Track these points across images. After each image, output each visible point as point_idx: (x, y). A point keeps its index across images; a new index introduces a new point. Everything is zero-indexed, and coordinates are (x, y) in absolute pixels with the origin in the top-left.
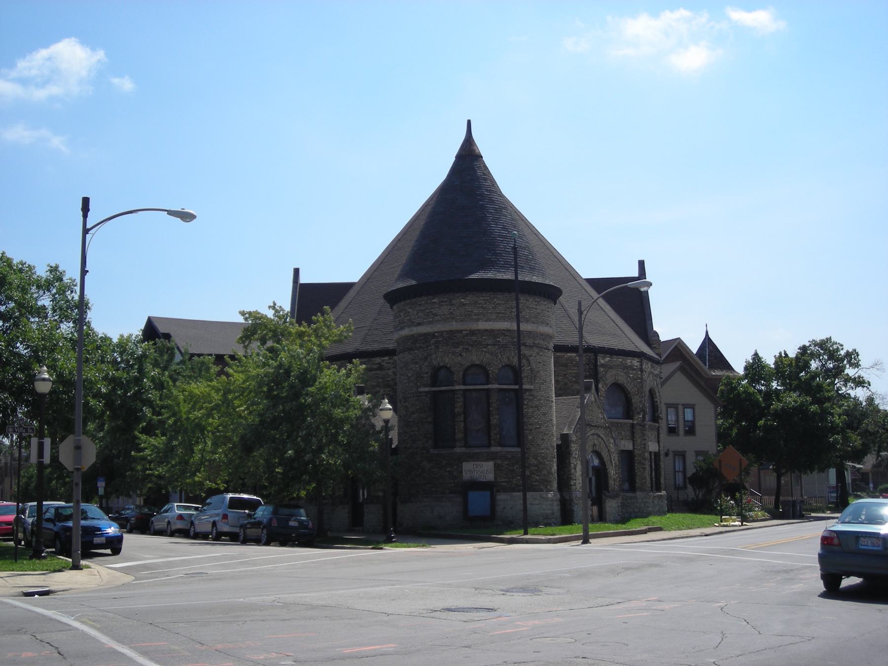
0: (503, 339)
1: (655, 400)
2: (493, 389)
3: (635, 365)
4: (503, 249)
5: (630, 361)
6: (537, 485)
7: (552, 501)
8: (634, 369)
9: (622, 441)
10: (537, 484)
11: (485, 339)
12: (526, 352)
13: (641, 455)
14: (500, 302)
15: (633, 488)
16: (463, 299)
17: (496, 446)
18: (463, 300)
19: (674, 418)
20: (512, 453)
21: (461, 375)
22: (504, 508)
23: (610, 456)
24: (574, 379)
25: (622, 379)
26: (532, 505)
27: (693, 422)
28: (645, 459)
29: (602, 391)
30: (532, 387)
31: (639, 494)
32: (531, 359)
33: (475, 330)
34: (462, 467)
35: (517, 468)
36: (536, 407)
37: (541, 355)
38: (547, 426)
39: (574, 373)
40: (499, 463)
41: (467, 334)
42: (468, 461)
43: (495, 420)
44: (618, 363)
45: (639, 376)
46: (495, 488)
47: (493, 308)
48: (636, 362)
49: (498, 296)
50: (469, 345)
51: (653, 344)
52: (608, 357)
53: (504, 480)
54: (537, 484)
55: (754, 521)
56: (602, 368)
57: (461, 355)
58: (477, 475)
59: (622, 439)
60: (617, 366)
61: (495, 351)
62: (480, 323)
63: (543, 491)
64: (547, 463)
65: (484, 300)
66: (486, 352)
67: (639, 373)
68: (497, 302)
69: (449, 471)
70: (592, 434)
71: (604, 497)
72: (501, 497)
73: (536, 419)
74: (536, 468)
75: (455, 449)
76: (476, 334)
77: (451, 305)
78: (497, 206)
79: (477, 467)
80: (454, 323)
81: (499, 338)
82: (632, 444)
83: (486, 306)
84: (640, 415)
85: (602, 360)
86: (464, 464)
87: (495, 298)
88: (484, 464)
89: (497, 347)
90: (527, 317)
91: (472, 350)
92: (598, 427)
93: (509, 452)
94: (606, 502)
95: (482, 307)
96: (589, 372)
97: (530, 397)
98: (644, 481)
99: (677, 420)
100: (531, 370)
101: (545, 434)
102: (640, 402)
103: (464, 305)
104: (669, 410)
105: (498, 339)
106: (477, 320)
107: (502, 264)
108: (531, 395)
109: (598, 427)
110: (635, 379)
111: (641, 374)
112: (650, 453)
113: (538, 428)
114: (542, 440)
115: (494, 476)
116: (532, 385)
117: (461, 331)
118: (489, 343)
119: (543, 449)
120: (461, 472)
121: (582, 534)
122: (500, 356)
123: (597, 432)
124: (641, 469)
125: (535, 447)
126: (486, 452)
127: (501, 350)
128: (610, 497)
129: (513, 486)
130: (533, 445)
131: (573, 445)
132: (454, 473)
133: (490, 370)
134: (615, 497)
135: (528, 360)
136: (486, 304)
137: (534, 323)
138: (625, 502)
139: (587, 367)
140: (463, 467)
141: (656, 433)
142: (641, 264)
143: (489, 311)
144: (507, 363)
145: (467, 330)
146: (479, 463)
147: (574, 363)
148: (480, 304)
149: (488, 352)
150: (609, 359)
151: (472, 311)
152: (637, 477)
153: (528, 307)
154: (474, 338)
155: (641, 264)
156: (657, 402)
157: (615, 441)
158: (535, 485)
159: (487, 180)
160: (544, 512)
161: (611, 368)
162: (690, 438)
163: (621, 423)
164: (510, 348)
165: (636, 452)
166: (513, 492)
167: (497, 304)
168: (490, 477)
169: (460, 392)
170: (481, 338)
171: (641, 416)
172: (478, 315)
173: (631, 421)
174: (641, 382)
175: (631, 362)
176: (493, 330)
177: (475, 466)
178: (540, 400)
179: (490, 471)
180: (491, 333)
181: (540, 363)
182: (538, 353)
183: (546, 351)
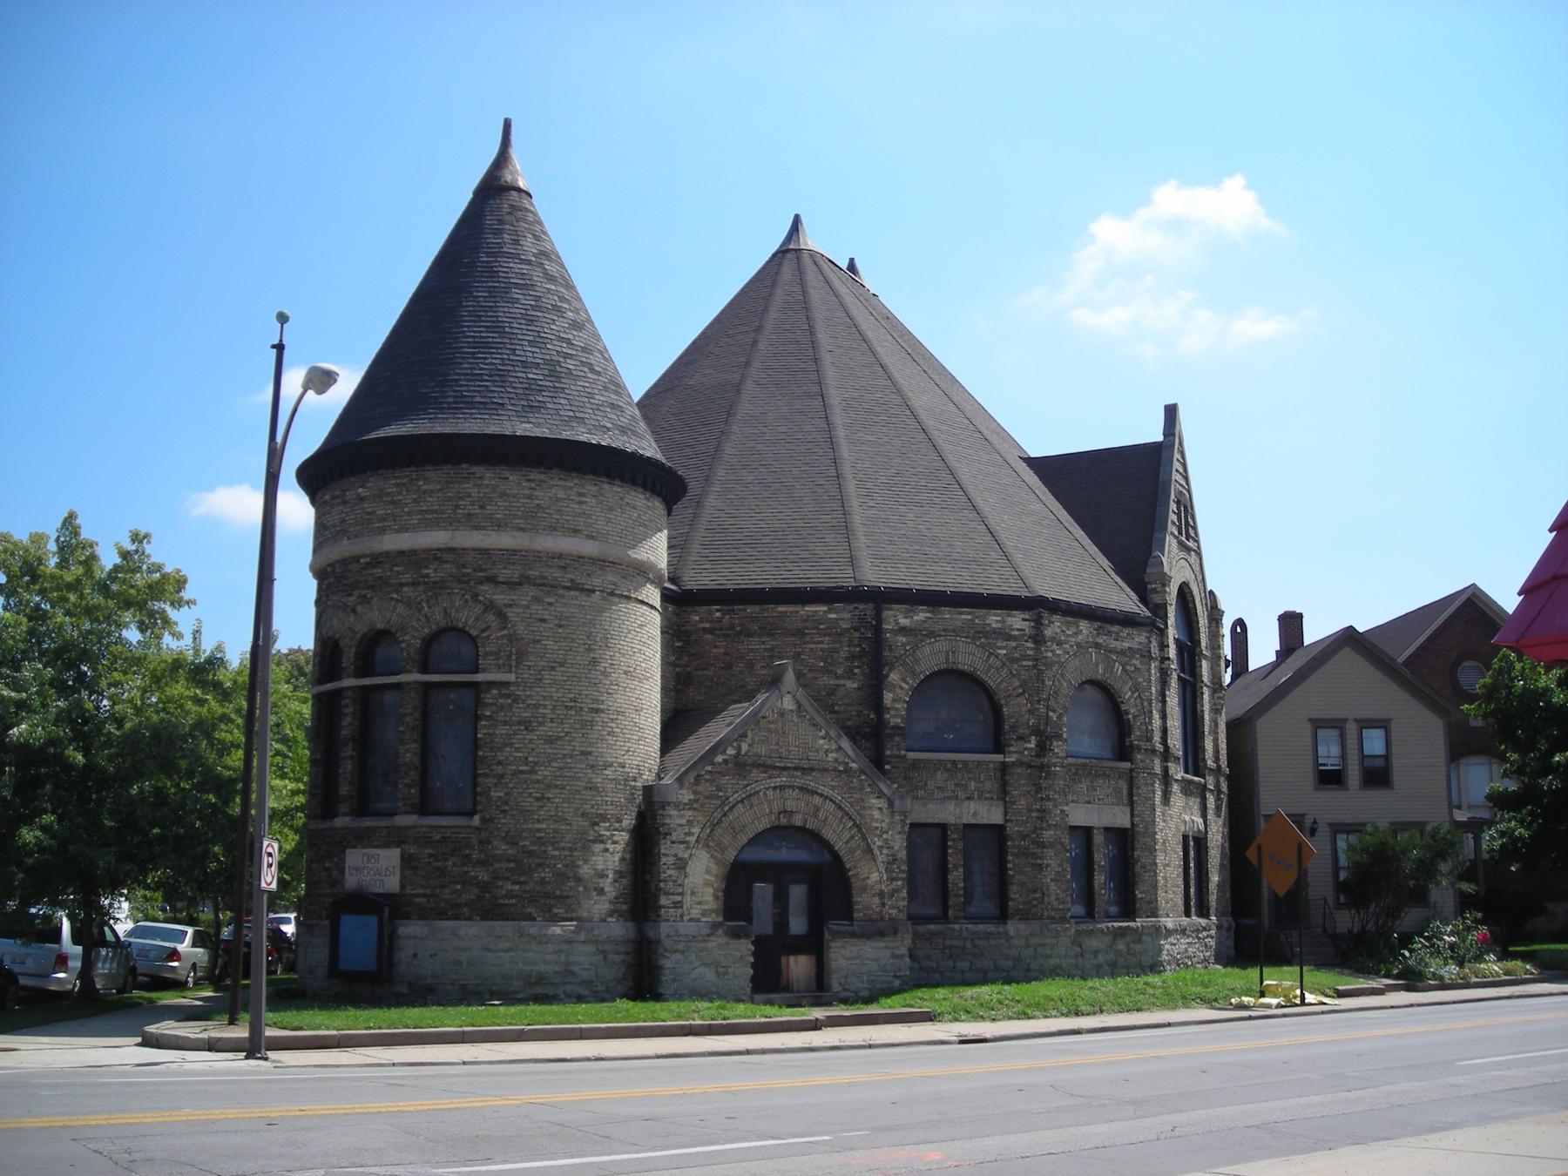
0: (435, 570)
1: (1123, 707)
2: (408, 683)
3: (1016, 627)
4: (469, 371)
5: (999, 618)
6: (511, 905)
7: (570, 942)
8: (1010, 638)
9: (966, 803)
10: (514, 901)
11: (399, 573)
12: (495, 597)
13: (1028, 836)
14: (431, 487)
15: (1003, 916)
16: (360, 487)
17: (408, 813)
18: (360, 490)
19: (1335, 750)
20: (445, 830)
21: (352, 655)
22: (415, 955)
23: (864, 838)
24: (822, 664)
25: (969, 658)
26: (489, 950)
27: (1387, 757)
28: (1042, 845)
29: (901, 688)
30: (511, 677)
31: (1012, 927)
32: (511, 614)
33: (381, 554)
34: (344, 861)
35: (454, 864)
36: (519, 723)
37: (550, 604)
38: (560, 768)
39: (822, 649)
41: (368, 564)
42: (355, 847)
43: (408, 755)
44: (959, 624)
45: (1029, 652)
47: (415, 501)
48: (1018, 622)
49: (428, 474)
50: (369, 588)
51: (1150, 583)
52: (921, 611)
53: (421, 891)
54: (514, 901)
55: (1443, 987)
56: (904, 636)
57: (354, 611)
59: (968, 799)
60: (954, 631)
61: (416, 597)
62: (386, 537)
63: (534, 919)
64: (556, 853)
65: (397, 485)
66: (397, 600)
67: (1030, 645)
68: (425, 487)
70: (775, 788)
71: (827, 936)
72: (410, 930)
73: (517, 750)
74: (512, 865)
75: (336, 819)
76: (381, 562)
77: (344, 503)
78: (499, 282)
79: (369, 861)
80: (345, 542)
81: (427, 567)
82: (1002, 809)
83: (401, 497)
84: (1030, 742)
85: (896, 617)
86: (348, 851)
87: (419, 480)
88: (383, 852)
89: (421, 588)
90: (499, 516)
91: (372, 598)
92: (805, 771)
93: (436, 827)
94: (829, 947)
95: (393, 502)
96: (859, 645)
97: (501, 701)
98: (1037, 895)
99: (1343, 756)
100: (512, 638)
101: (549, 786)
102: (1031, 712)
103: (362, 499)
104: (1321, 732)
105: (426, 571)
106: (382, 531)
107: (449, 403)
108: (508, 696)
109: (805, 771)
110: (1013, 660)
111: (1037, 649)
112: (1084, 834)
113: (522, 772)
114: (538, 799)
115: (401, 882)
116: (510, 672)
117: (356, 559)
118: (403, 581)
119: (539, 821)
120: (342, 871)
121: (247, 1035)
122: (426, 609)
123: (799, 782)
124: (1027, 869)
125: (513, 816)
127: (430, 594)
128: (853, 935)
129: (442, 905)
130: (504, 812)
131: (674, 813)
133: (403, 642)
134: (878, 930)
135: (501, 615)
136: (400, 493)
137: (522, 529)
138: (969, 945)
139: (857, 634)
140: (347, 860)
141: (1123, 785)
142: (1171, 412)
143: (406, 510)
144: (443, 624)
145: (366, 556)
146: (374, 851)
147: (821, 627)
148: (389, 494)
149: (402, 601)
150: (928, 615)
151: (373, 513)
152: (1015, 888)
153: (503, 495)
154: (378, 571)
155: (1171, 412)
156: (1127, 713)
157: (891, 804)
158: (503, 905)
159: (501, 234)
160: (528, 968)
161: (932, 634)
162: (1376, 796)
163: (965, 763)
164: (448, 588)
165: (1012, 829)
167: (425, 492)
168: (392, 884)
169: (350, 693)
170: (391, 570)
171: (1033, 746)
172: (384, 520)
173: (999, 758)
174: (1035, 666)
175: (1003, 621)
176: (415, 551)
178: (537, 706)
179: (391, 869)
180: (411, 558)
181: (543, 620)
182: (536, 599)
183: (572, 593)
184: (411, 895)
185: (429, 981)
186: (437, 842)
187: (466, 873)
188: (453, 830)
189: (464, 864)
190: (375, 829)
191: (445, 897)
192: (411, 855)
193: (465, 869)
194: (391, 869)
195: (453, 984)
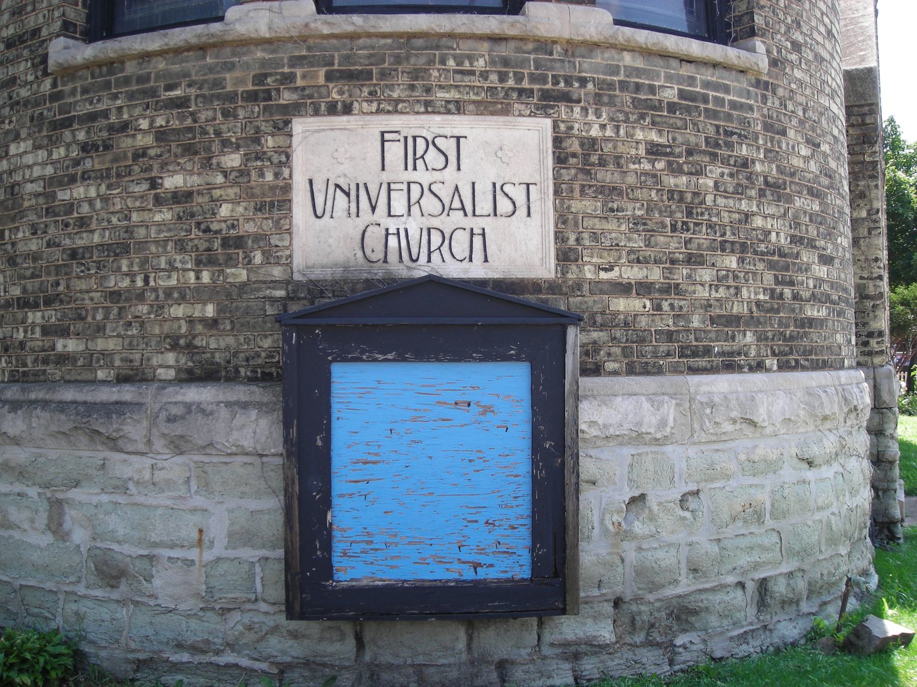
10: (823, 313)
20: (686, 70)
22: (638, 501)
34: (286, 155)
40: (595, 132)
46: (573, 335)
53: (633, 274)
58: (414, 225)
69: (181, 197)
93: (665, 56)
115: (560, 237)
126: (496, 39)
132: (225, 210)
166: (693, 370)
177: (395, 151)
179: (519, 194)
184: (598, 287)
185: (685, 585)
186: (672, 107)
187: (747, 216)
188: (709, 75)
189: (739, 192)
190: (434, 40)
191: (703, 293)
192: (591, 144)
193: (744, 206)
194: (519, 194)
195: (741, 585)
